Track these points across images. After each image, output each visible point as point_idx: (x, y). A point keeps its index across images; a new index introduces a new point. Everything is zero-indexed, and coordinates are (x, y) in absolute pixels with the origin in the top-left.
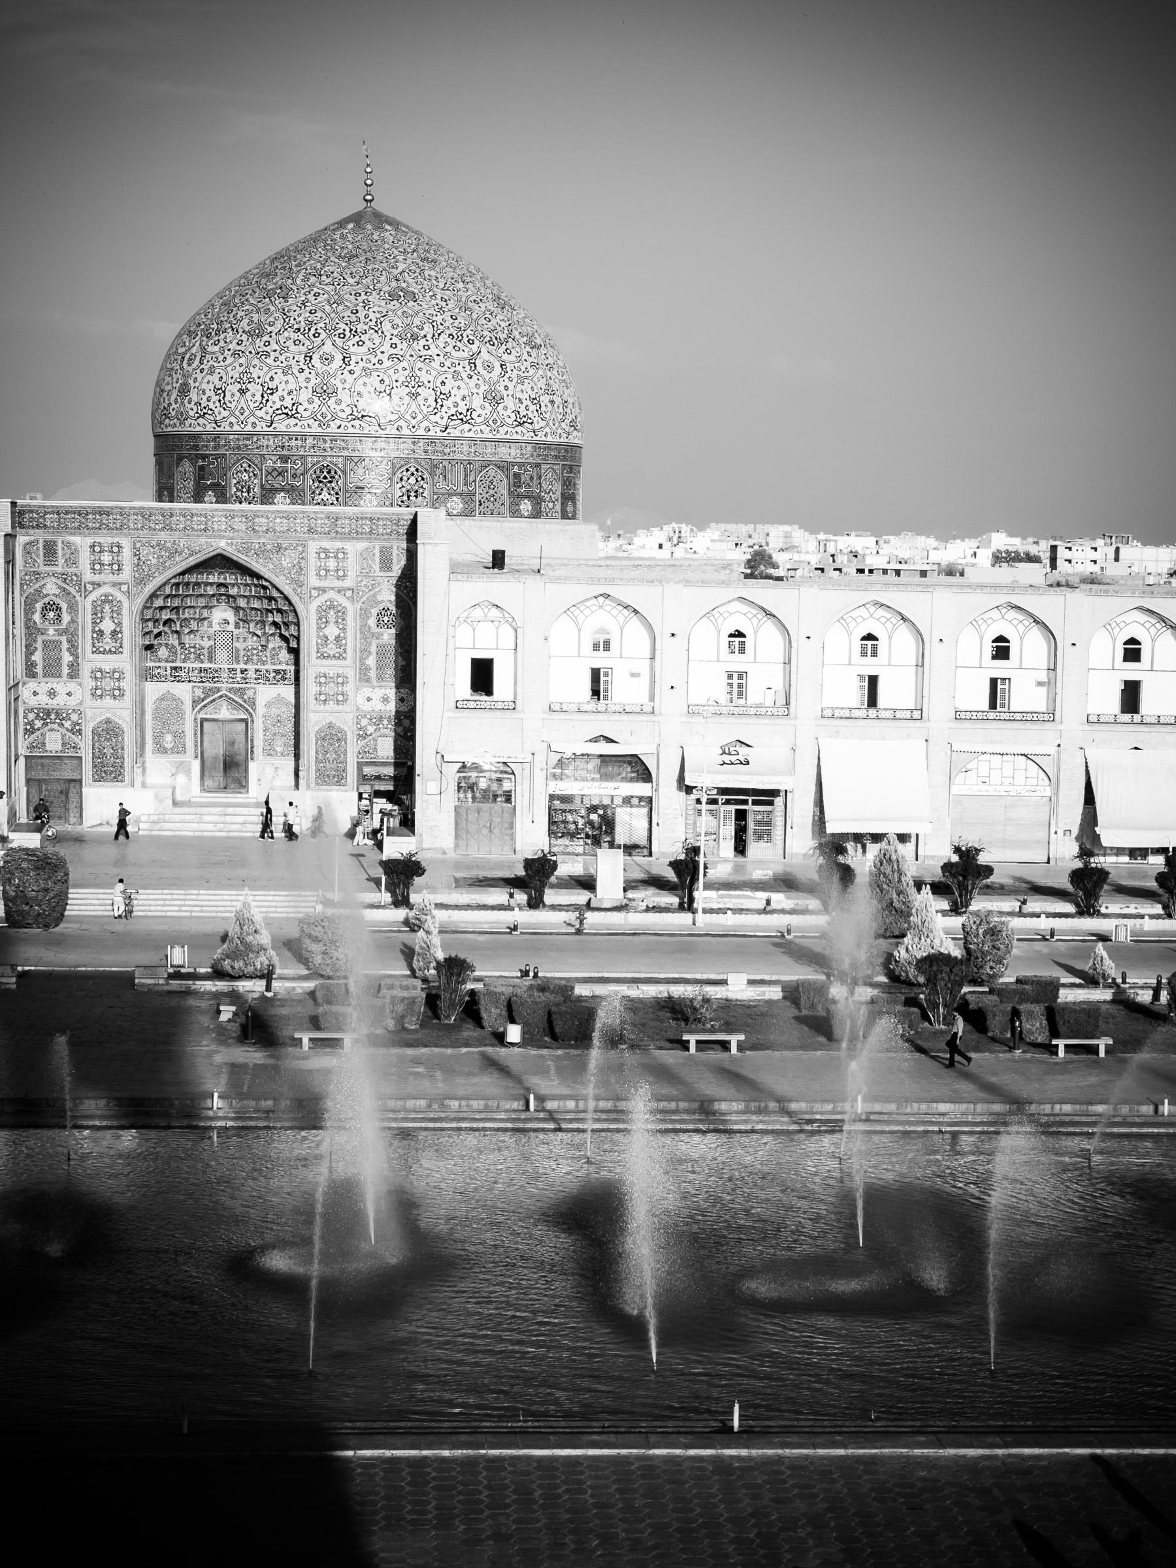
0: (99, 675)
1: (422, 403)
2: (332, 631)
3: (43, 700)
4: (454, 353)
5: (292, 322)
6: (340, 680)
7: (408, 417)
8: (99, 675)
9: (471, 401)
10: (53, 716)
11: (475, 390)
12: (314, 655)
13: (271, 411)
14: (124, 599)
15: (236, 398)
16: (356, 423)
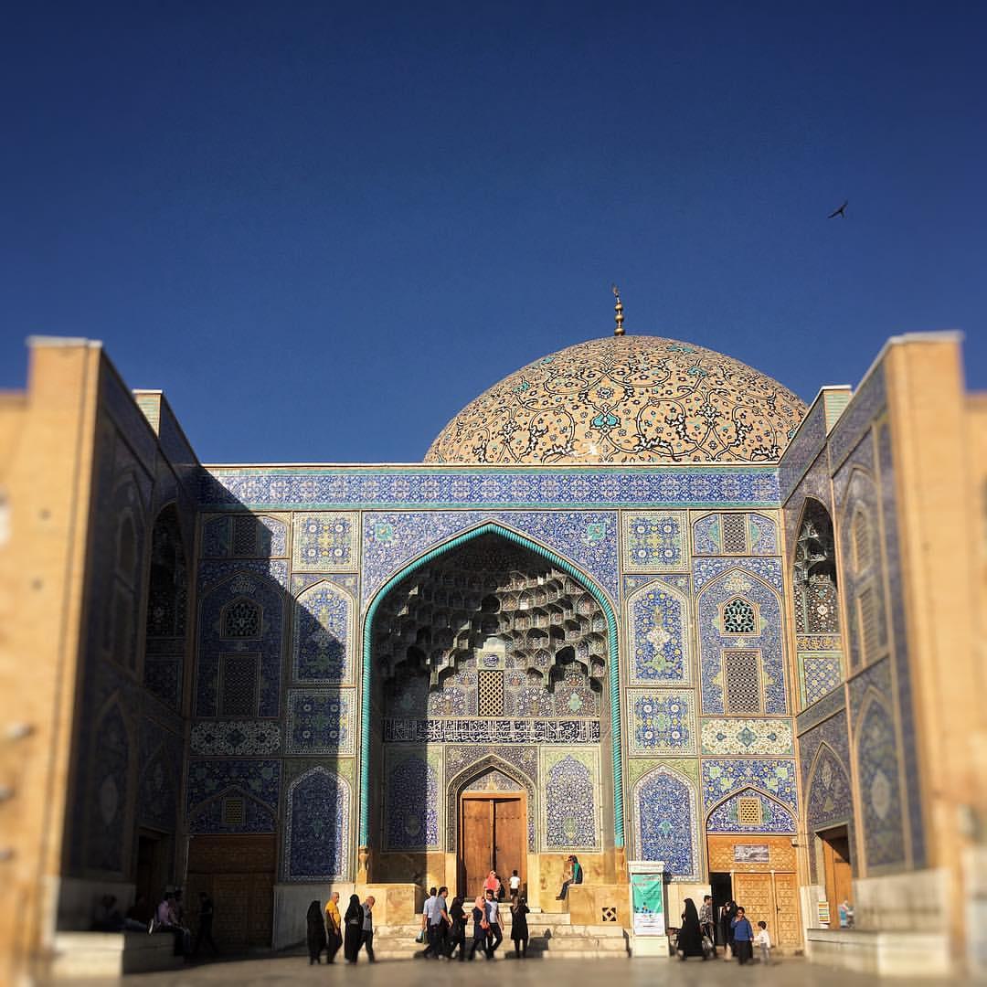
0: (307, 708)
1: (721, 433)
2: (659, 636)
3: (223, 746)
4: (748, 391)
5: (561, 371)
6: (675, 708)
7: (706, 446)
8: (307, 708)
9: (775, 437)
10: (234, 774)
11: (778, 429)
12: (633, 675)
13: (540, 453)
14: (348, 598)
15: (498, 451)
16: (645, 454)
